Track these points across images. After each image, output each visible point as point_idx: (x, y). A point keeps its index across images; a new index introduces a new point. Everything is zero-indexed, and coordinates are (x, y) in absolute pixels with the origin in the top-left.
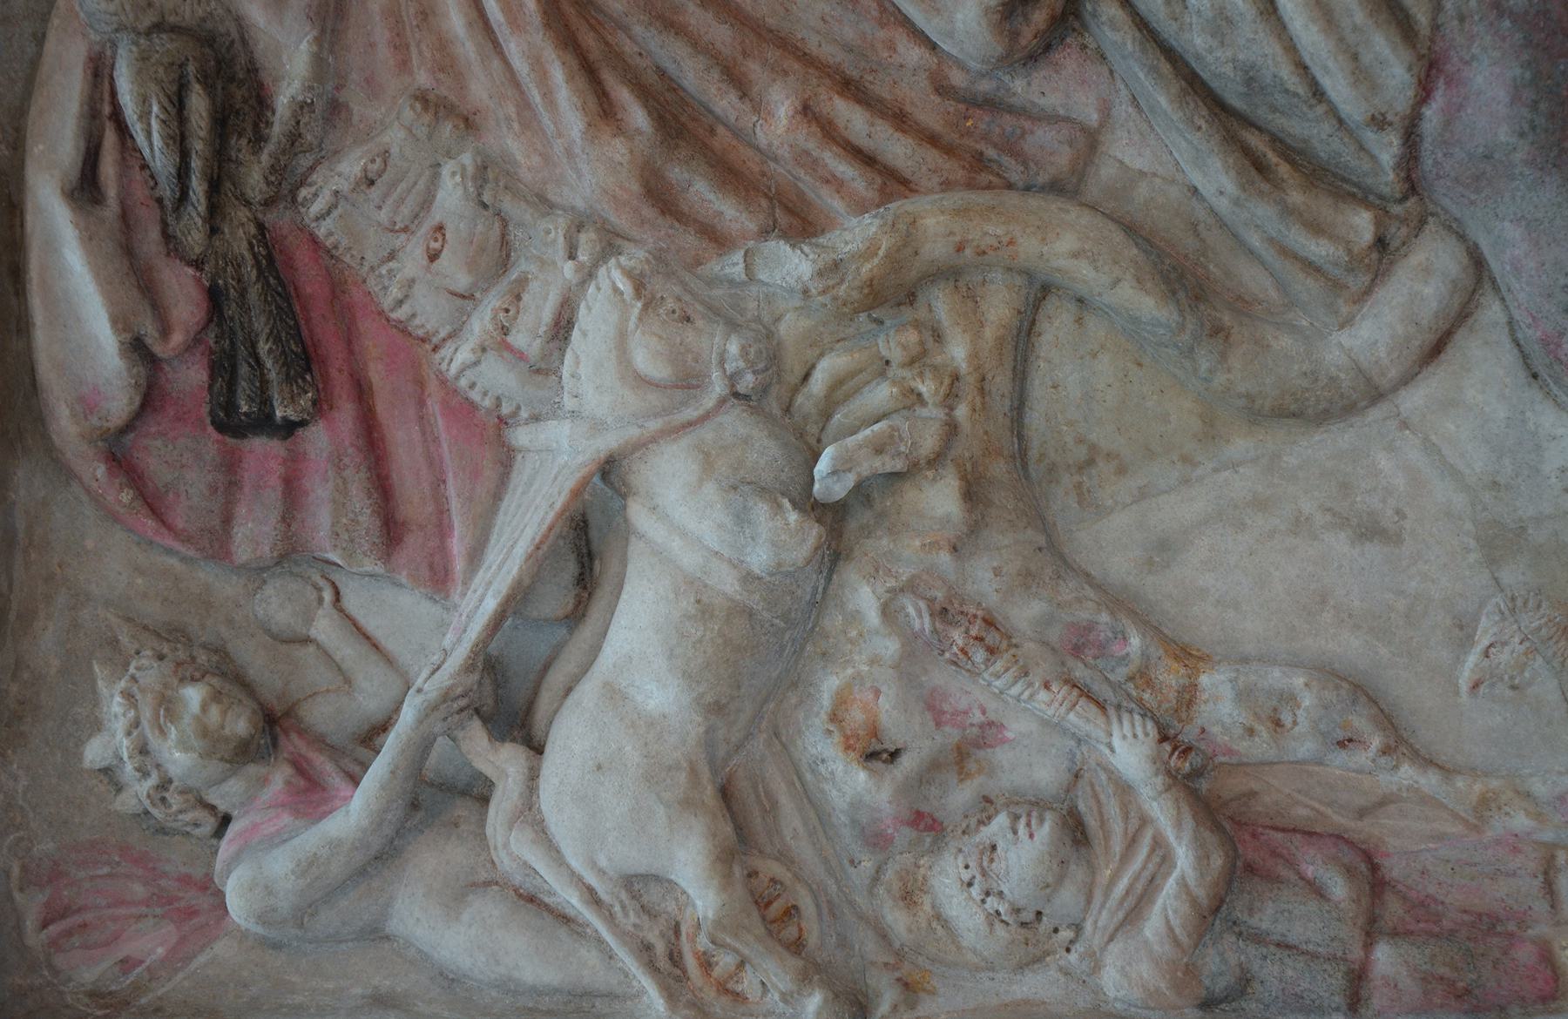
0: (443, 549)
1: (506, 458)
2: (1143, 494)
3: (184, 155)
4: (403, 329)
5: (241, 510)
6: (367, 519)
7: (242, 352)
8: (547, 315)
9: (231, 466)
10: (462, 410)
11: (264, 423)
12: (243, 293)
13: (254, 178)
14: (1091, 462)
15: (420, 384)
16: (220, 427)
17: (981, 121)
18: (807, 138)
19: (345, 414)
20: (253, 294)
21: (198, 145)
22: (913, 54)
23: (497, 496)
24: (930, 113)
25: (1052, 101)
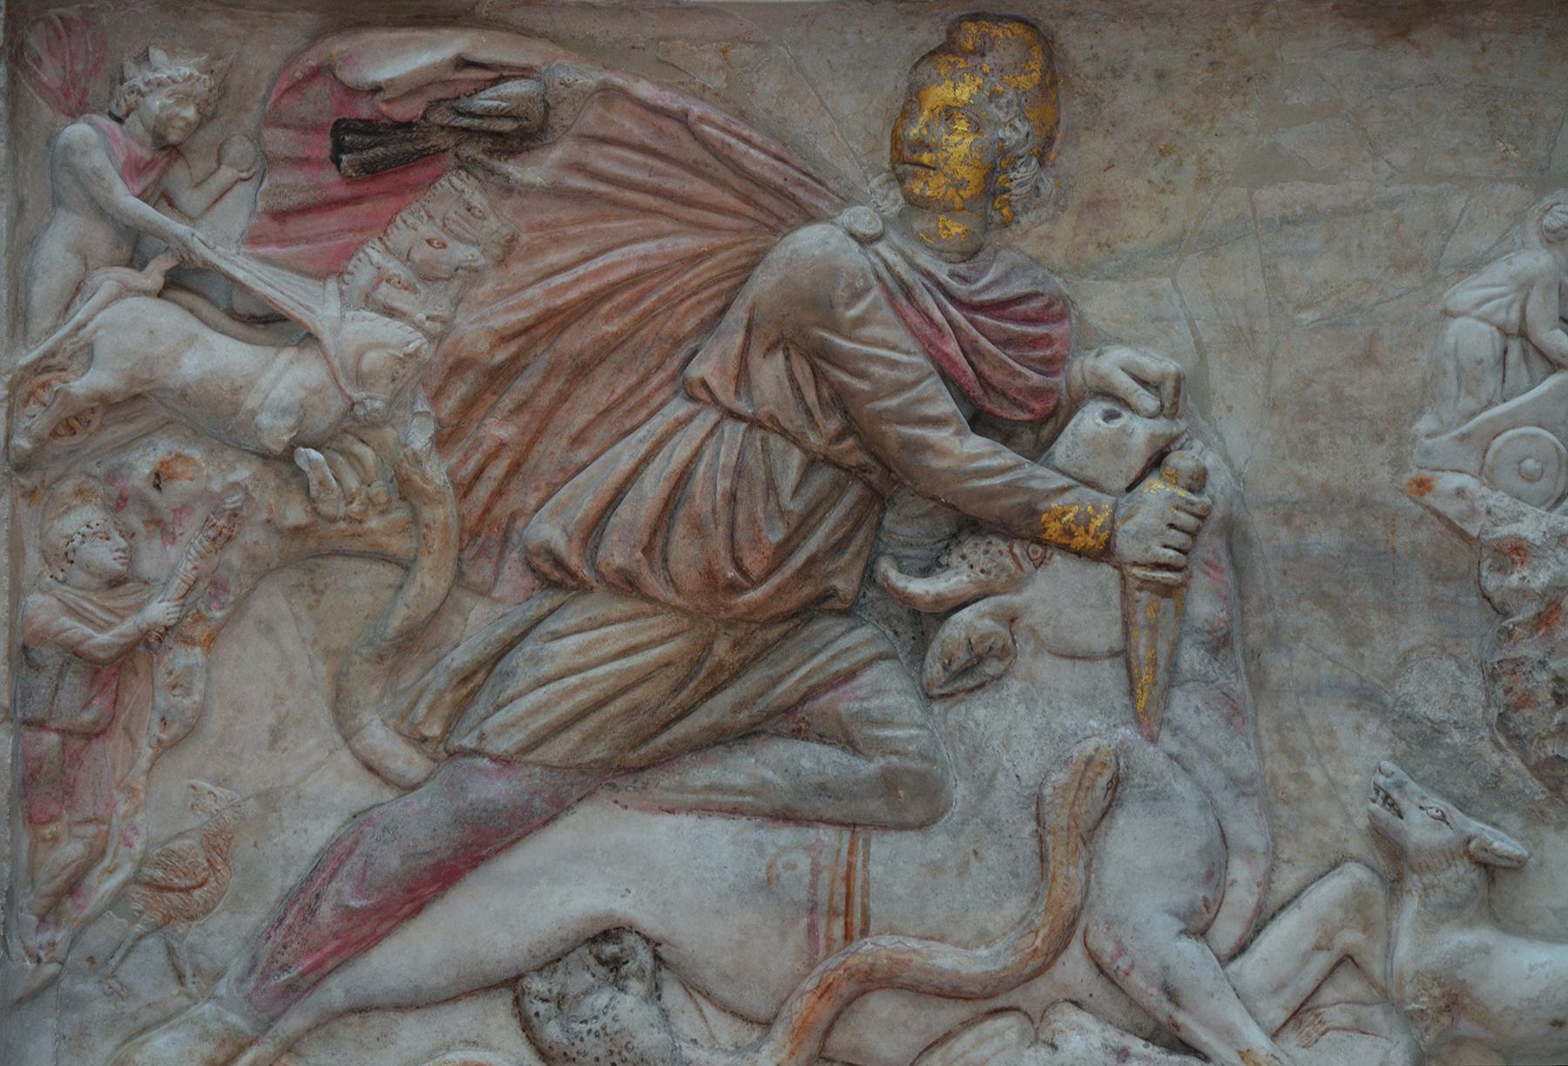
0: (269, 242)
1: (320, 277)
2: (297, 619)
3: (481, 117)
4: (391, 221)
5: (292, 134)
6: (287, 203)
7: (378, 139)
8: (397, 304)
9: (316, 128)
10: (347, 253)
11: (339, 149)
12: (409, 140)
13: (471, 151)
14: (315, 591)
15: (362, 230)
16: (337, 123)
17: (497, 535)
18: (488, 445)
19: (344, 192)
20: (408, 147)
21: (485, 124)
22: (532, 500)
23: (299, 272)
24: (501, 510)
25: (506, 572)
